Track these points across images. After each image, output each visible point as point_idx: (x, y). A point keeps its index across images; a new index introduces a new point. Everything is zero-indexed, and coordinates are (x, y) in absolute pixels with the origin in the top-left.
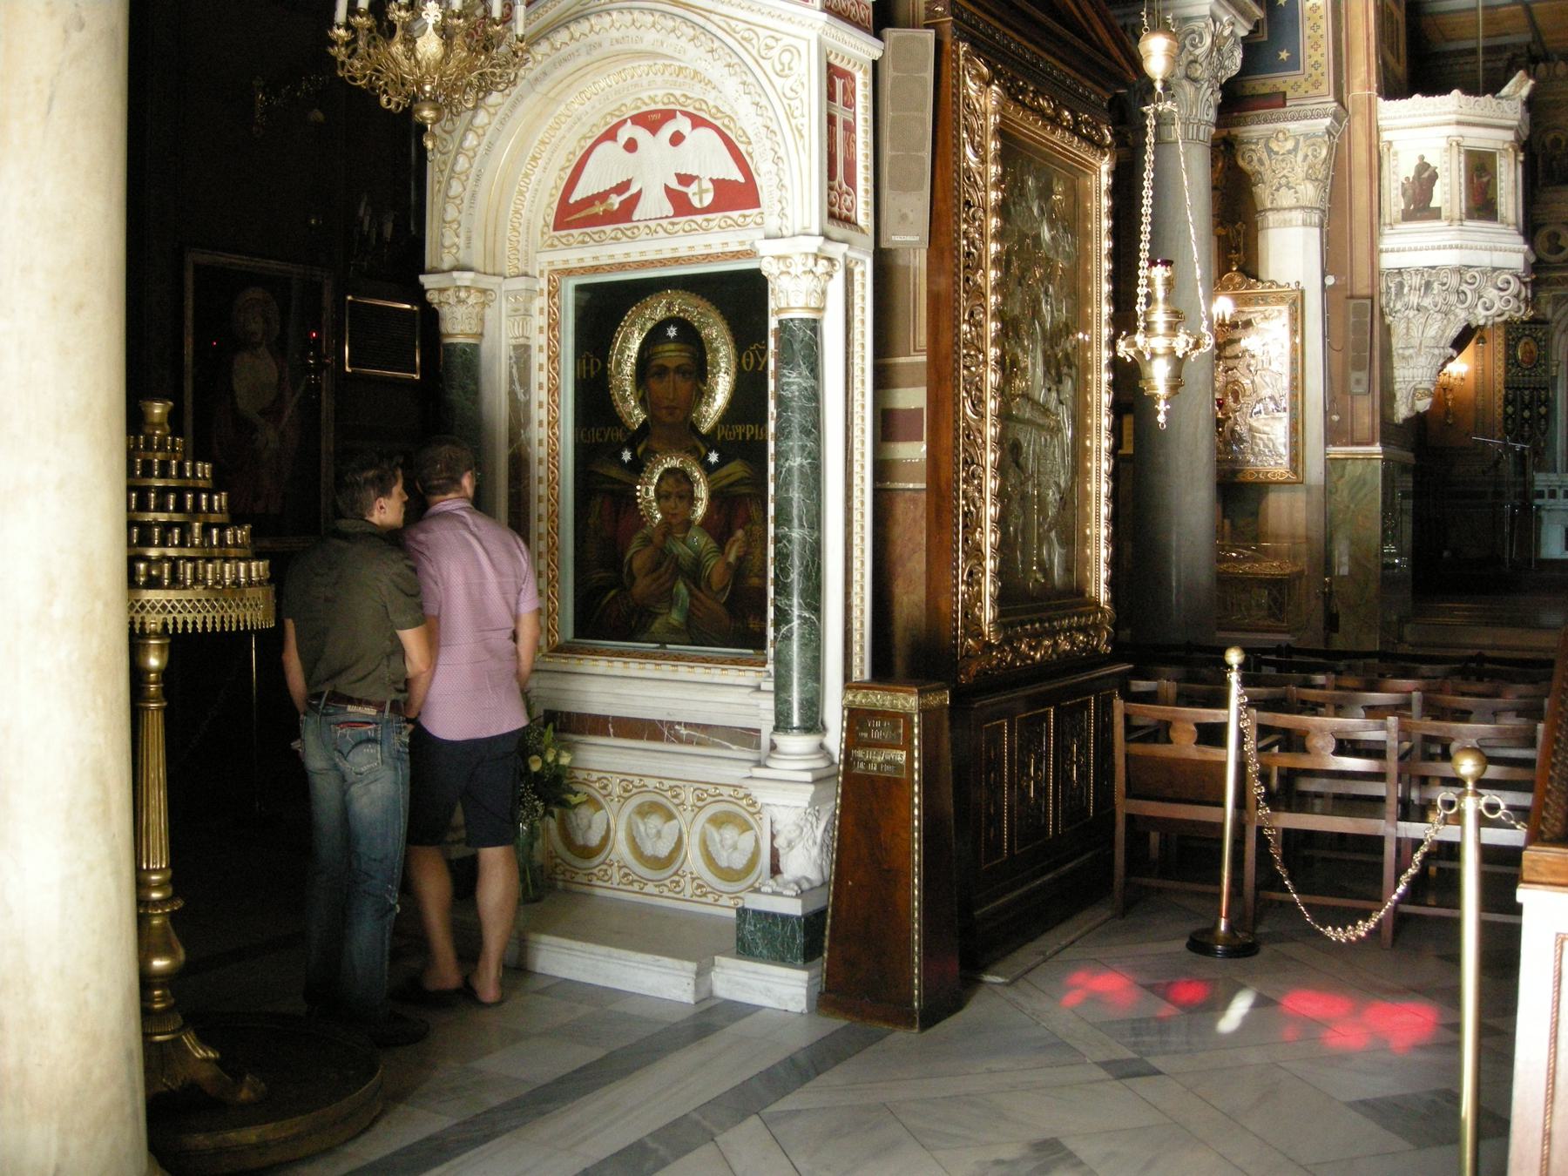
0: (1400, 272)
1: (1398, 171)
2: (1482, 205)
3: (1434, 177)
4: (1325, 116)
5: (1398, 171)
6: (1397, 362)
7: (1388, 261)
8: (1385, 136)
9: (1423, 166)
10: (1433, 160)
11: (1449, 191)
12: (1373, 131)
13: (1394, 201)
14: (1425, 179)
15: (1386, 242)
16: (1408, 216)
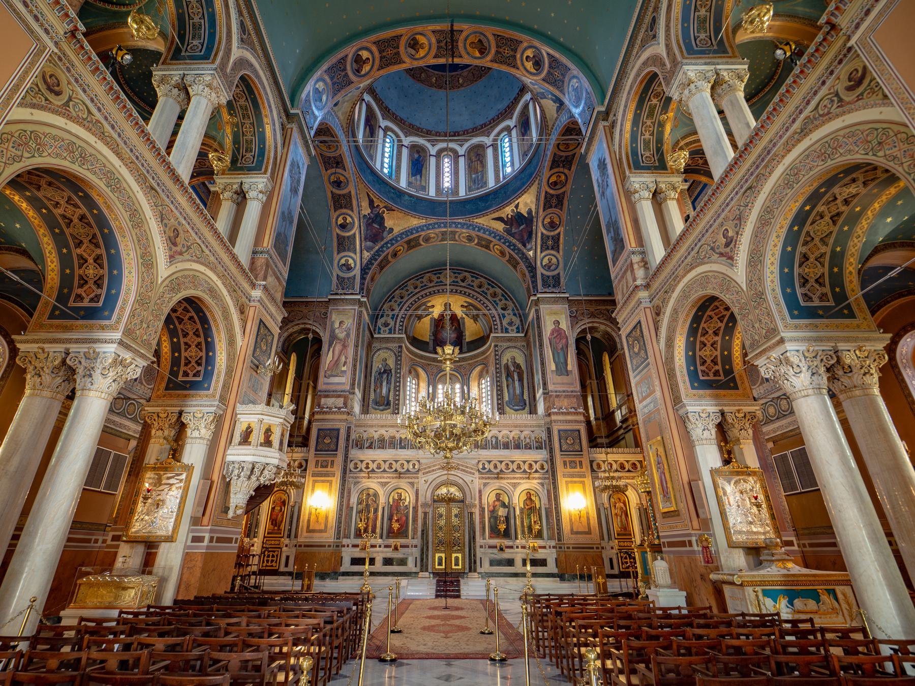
0: (233, 463)
1: (240, 428)
2: (268, 443)
3: (251, 431)
4: (212, 406)
5: (240, 428)
6: (232, 495)
7: (229, 458)
8: (238, 416)
9: (249, 427)
10: (252, 425)
11: (257, 436)
12: (234, 414)
13: (237, 438)
14: (248, 433)
15: (229, 452)
16: (240, 444)
